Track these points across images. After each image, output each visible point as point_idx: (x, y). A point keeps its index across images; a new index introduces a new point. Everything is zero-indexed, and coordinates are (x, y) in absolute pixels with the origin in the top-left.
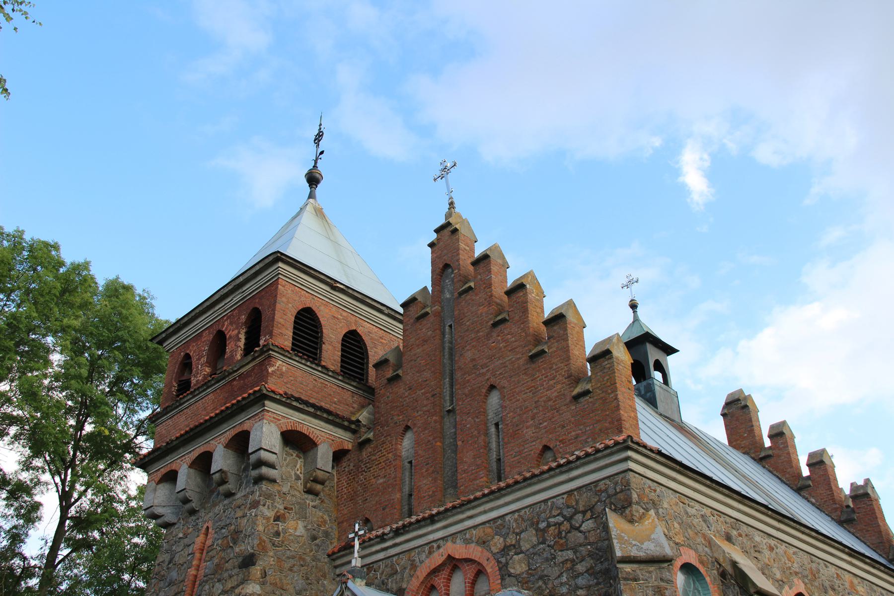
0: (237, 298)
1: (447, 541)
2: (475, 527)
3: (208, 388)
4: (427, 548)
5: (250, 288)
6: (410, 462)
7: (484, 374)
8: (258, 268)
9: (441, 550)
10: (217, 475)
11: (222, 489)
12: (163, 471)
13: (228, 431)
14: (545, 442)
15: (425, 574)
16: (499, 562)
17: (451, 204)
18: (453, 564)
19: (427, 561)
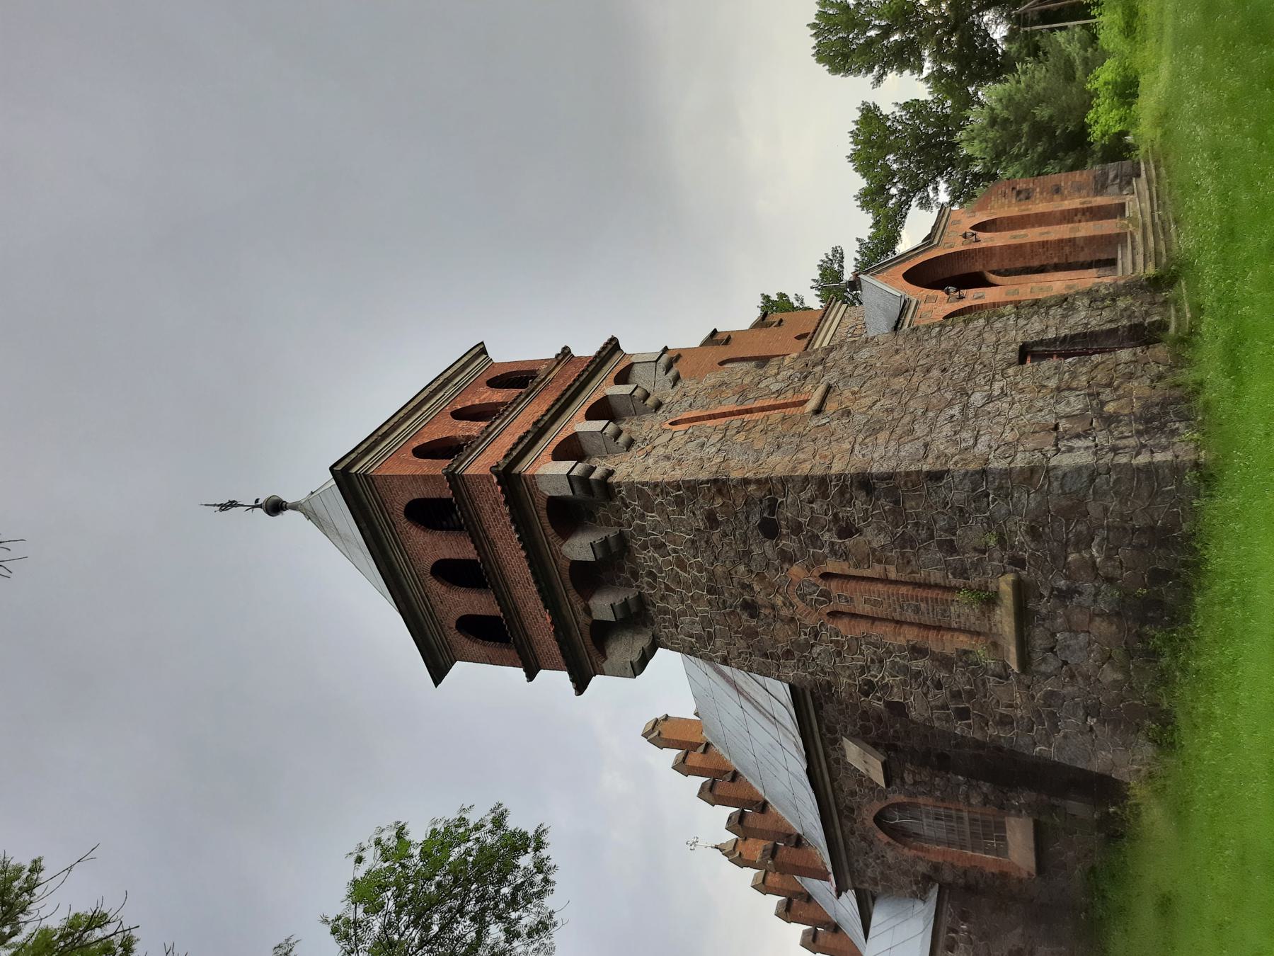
0: (450, 389)
8: (465, 359)
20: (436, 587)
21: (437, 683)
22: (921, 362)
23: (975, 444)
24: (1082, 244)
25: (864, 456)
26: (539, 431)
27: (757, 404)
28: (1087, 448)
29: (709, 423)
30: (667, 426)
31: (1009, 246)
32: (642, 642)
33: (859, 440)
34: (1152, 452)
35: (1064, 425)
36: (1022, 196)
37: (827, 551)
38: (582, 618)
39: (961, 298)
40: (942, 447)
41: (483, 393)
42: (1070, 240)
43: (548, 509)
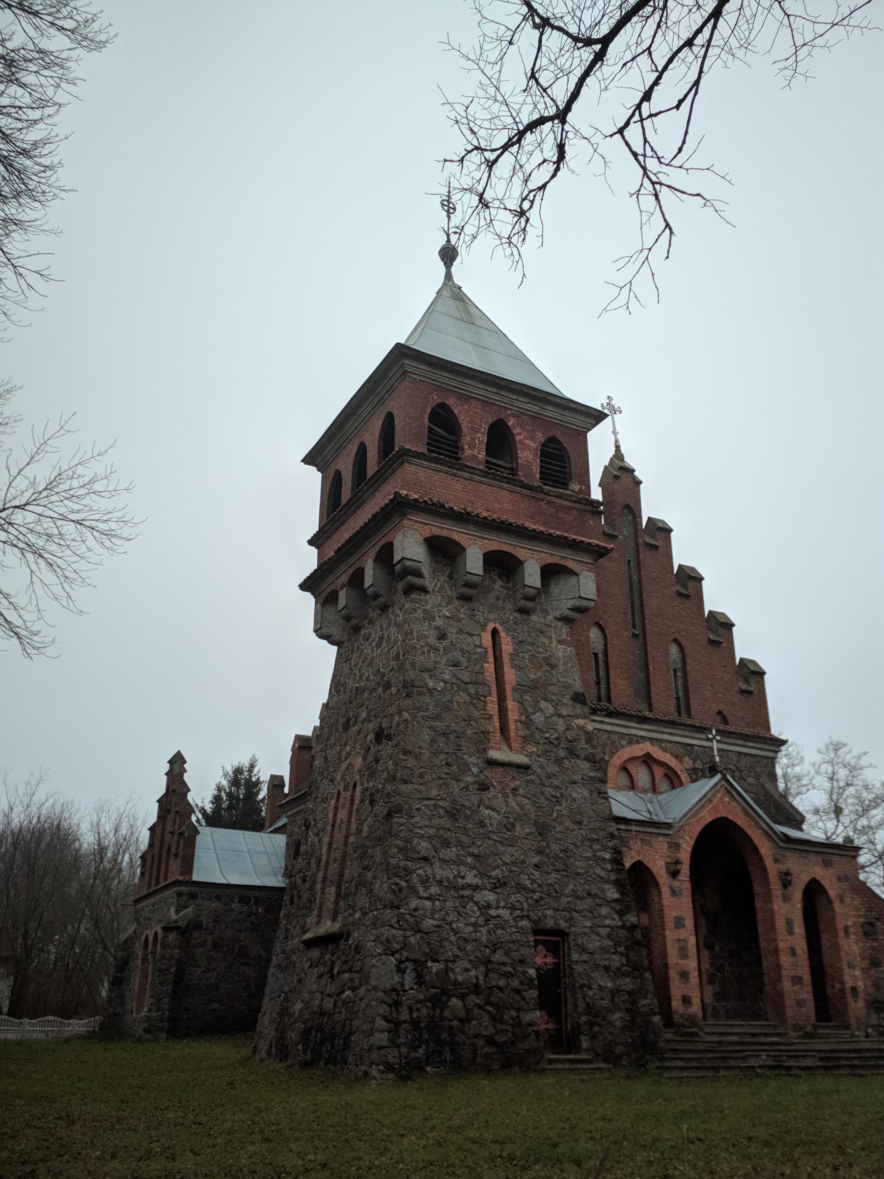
1: (645, 741)
2: (670, 742)
3: (507, 483)
4: (627, 737)
5: (550, 412)
6: (596, 655)
7: (668, 626)
9: (641, 746)
10: (532, 590)
11: (523, 603)
12: (438, 532)
13: (555, 556)
14: (720, 708)
15: (626, 757)
16: (689, 775)
17: (618, 448)
18: (648, 760)
19: (628, 748)
20: (353, 448)
21: (302, 461)
22: (554, 846)
23: (421, 898)
24: (779, 988)
25: (419, 809)
26: (463, 518)
27: (511, 705)
28: (402, 984)
29: (490, 667)
30: (491, 626)
31: (773, 918)
32: (336, 632)
33: (441, 803)
34: (389, 1032)
35: (434, 967)
36: (868, 927)
37: (366, 785)
38: (340, 582)
39: (674, 874)
40: (421, 872)
41: (533, 439)
42: (780, 976)
43: (388, 543)
